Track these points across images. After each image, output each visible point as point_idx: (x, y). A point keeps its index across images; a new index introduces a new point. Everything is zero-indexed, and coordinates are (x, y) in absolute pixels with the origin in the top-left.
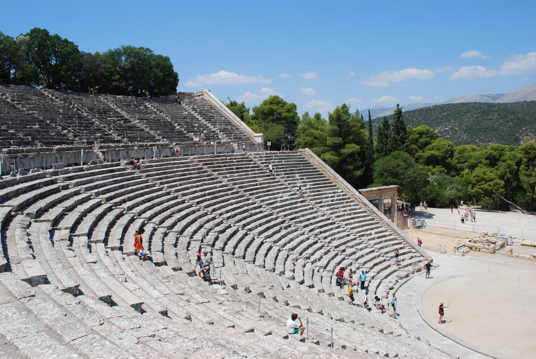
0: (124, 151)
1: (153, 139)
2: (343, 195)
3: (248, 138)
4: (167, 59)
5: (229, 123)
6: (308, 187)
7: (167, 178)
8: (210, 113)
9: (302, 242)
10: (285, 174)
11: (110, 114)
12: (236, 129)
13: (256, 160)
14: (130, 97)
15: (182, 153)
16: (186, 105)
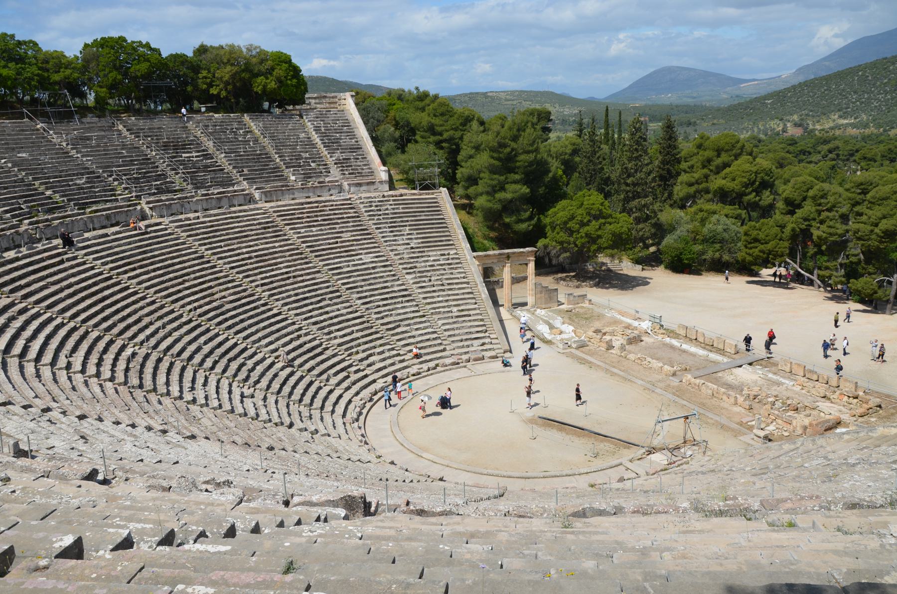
0: (178, 205)
1: (229, 182)
2: (453, 259)
3: (372, 172)
4: (284, 60)
5: (357, 148)
6: (412, 245)
7: (214, 237)
8: (338, 133)
9: (336, 317)
10: (390, 227)
11: (190, 148)
12: (362, 158)
13: (362, 206)
14: (232, 115)
15: (264, 199)
16: (309, 121)
